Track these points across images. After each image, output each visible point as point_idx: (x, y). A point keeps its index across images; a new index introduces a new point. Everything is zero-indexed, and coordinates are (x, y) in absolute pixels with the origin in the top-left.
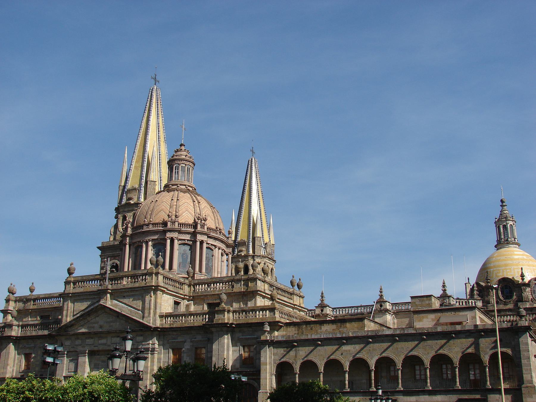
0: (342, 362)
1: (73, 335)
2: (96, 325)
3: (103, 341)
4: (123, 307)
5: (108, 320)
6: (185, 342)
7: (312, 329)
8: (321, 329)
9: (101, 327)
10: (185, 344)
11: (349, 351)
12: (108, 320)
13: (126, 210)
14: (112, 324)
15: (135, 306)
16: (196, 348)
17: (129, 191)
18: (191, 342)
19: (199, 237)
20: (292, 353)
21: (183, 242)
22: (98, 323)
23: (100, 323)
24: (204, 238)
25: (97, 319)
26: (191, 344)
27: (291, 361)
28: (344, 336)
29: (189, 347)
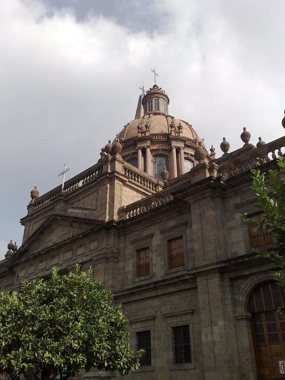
1: (26, 261)
4: (77, 213)
6: (152, 235)
10: (154, 238)
15: (90, 207)
16: (169, 241)
19: (174, 144)
21: (157, 153)
24: (181, 145)
25: (52, 236)
29: (159, 242)
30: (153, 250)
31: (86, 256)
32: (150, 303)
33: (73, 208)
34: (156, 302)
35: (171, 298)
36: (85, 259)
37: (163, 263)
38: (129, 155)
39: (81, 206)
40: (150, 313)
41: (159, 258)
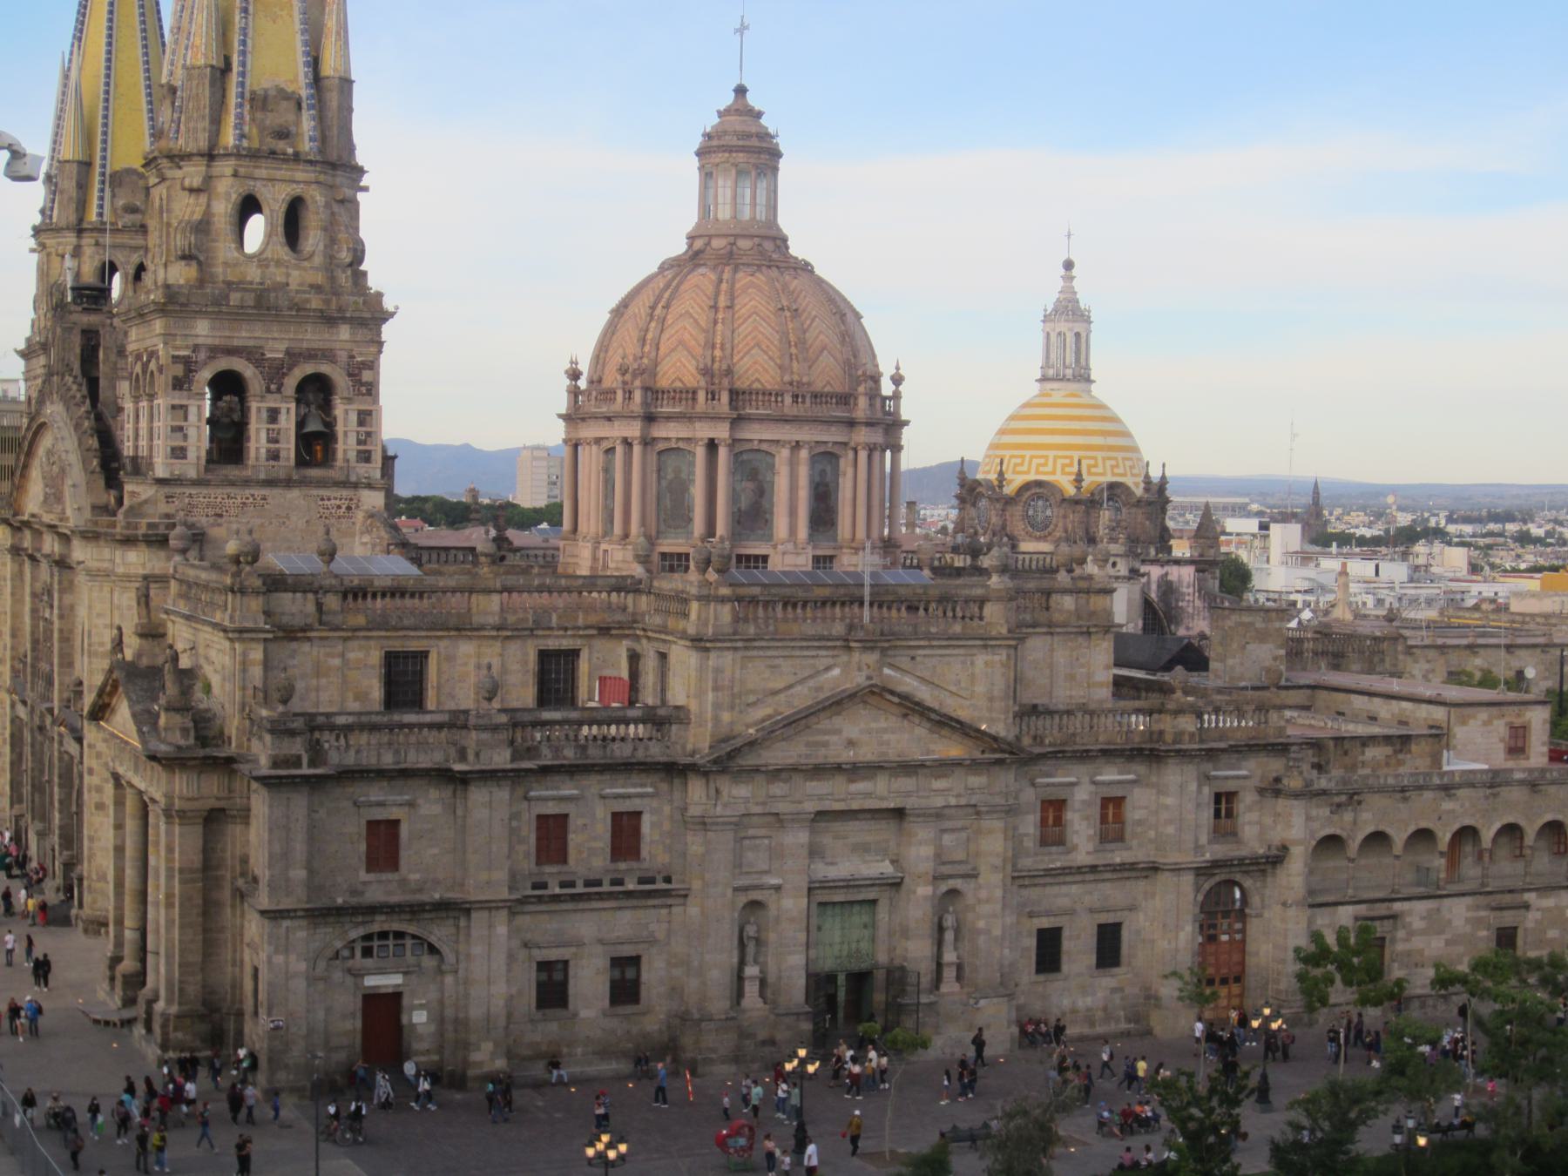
0: (1439, 834)
2: (834, 738)
3: (861, 786)
5: (874, 725)
7: (1346, 753)
8: (1363, 753)
9: (851, 743)
10: (1076, 789)
11: (1453, 811)
12: (874, 725)
13: (263, 173)
14: (886, 737)
15: (953, 689)
17: (260, 102)
18: (1094, 783)
20: (1348, 816)
22: (838, 732)
23: (871, 734)
25: (837, 721)
26: (1093, 788)
27: (1344, 834)
28: (1446, 780)
29: (1085, 797)
30: (1077, 805)
31: (958, 796)
32: (1064, 889)
33: (891, 666)
34: (1074, 889)
35: (1101, 886)
36: (953, 801)
37: (1091, 832)
38: (826, 443)
39: (926, 674)
40: (1064, 902)
41: (1085, 823)
